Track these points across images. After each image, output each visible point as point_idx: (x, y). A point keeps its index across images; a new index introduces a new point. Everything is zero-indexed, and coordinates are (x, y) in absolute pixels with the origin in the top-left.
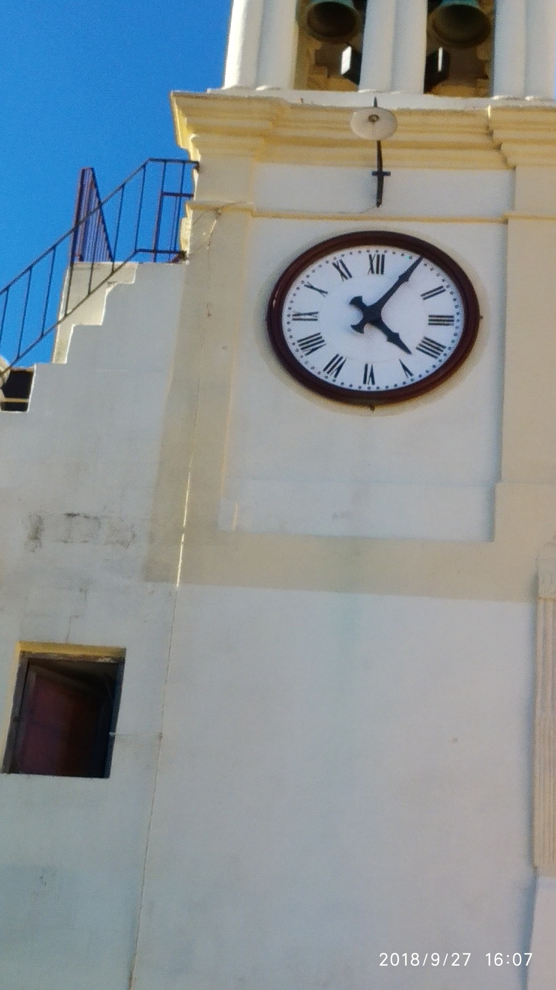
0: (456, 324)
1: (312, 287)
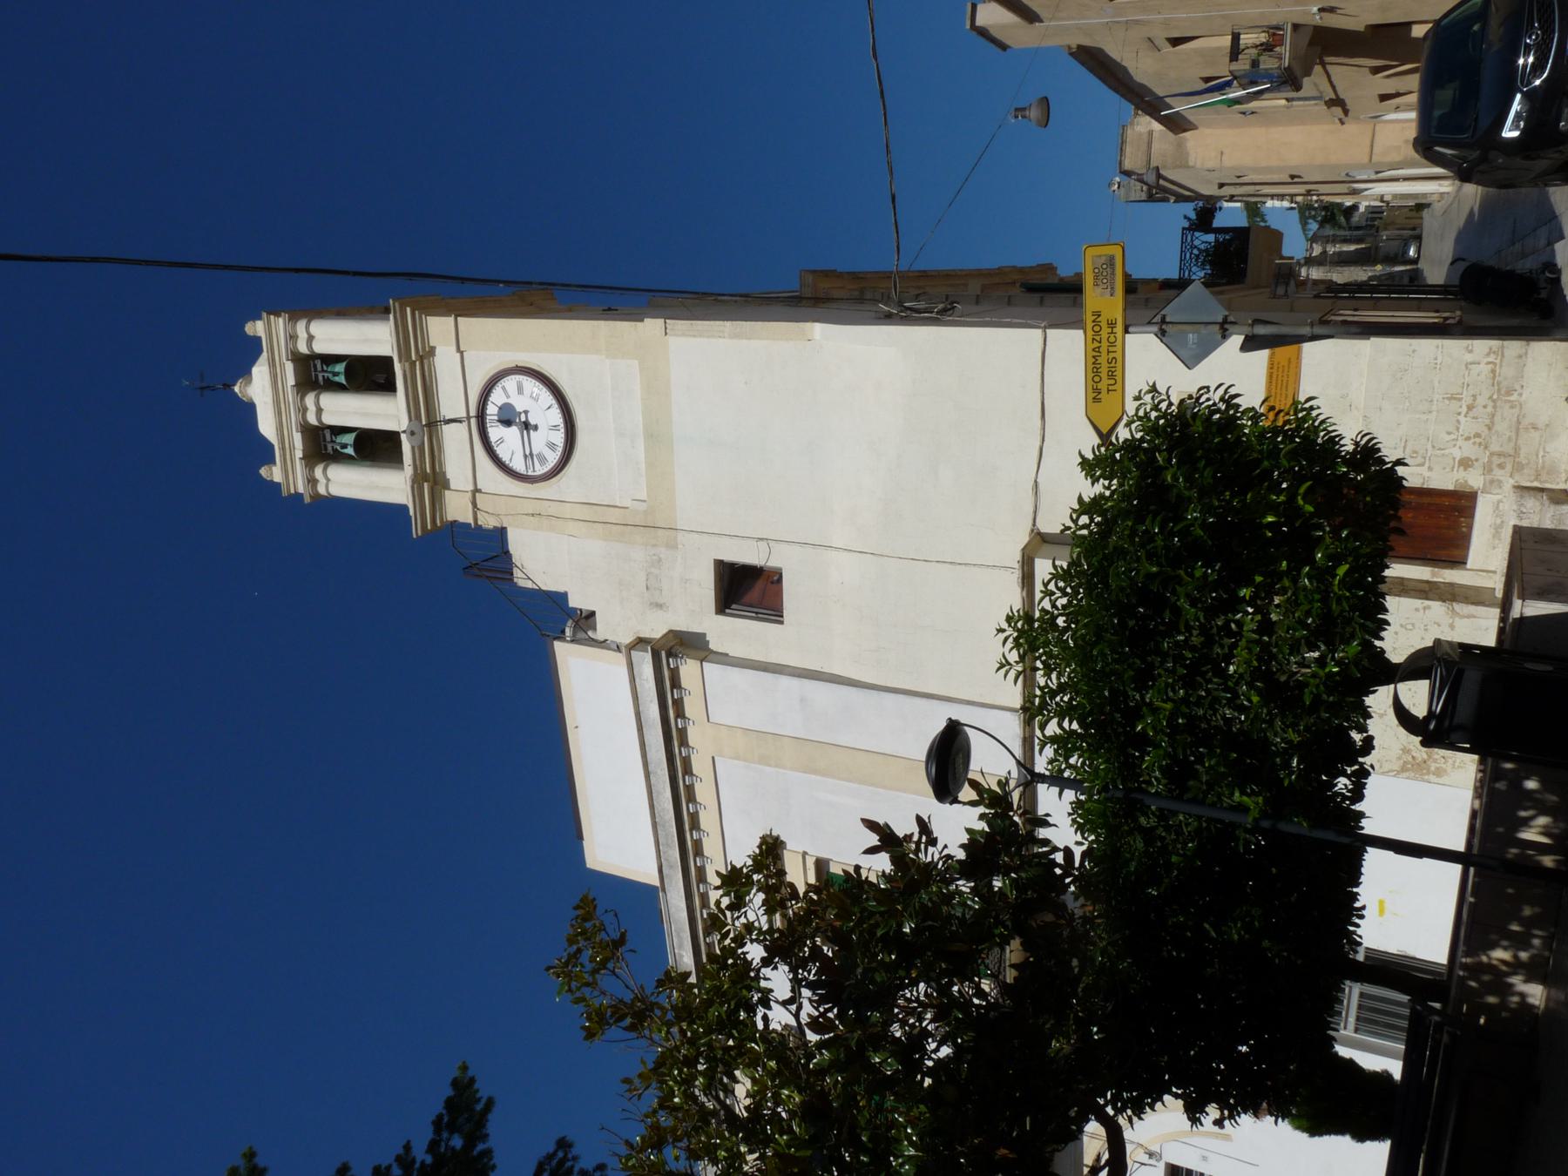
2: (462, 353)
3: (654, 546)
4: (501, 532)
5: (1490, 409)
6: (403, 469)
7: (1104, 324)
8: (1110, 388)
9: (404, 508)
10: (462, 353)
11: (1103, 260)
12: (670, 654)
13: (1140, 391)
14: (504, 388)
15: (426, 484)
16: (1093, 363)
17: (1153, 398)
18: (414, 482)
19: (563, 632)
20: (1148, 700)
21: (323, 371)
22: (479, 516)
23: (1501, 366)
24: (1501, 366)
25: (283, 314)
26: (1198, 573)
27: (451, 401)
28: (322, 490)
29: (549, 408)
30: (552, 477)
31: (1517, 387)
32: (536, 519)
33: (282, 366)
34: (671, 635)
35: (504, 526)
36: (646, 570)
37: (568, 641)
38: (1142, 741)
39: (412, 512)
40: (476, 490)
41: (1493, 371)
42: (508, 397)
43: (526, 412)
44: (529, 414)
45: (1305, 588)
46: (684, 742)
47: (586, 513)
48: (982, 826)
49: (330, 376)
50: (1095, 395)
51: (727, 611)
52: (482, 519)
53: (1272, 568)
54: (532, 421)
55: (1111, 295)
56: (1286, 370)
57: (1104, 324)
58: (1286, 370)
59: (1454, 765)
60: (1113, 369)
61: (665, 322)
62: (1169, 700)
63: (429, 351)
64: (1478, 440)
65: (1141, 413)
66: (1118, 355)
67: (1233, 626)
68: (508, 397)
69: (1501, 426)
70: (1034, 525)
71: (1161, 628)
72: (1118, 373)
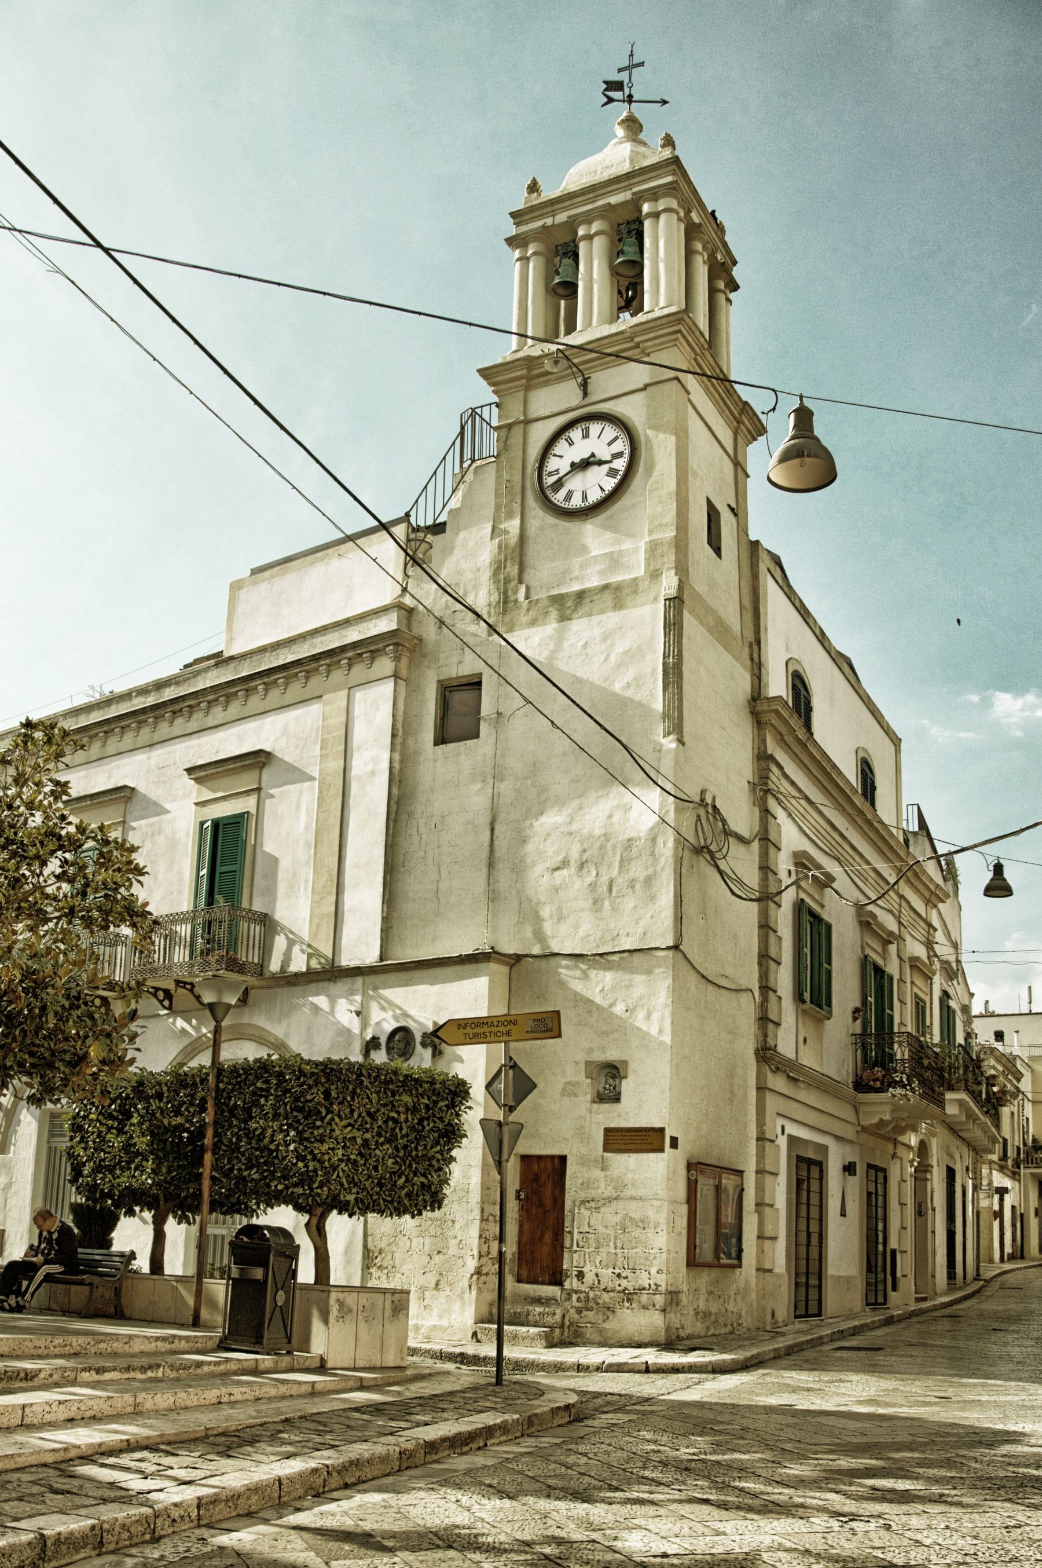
14: (616, 438)
33: (628, 187)
41: (644, 1289)
57: (508, 1028)
69: (606, 1297)
72: (476, 1040)
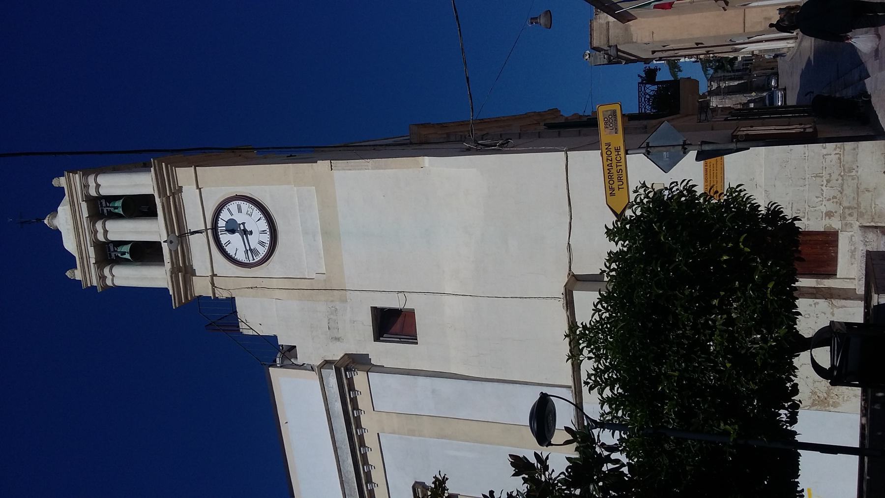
0: (240, 203)
1: (236, 254)
2: (200, 189)
3: (332, 301)
4: (232, 300)
5: (840, 181)
6: (164, 265)
7: (613, 150)
8: (620, 187)
9: (167, 290)
10: (200, 189)
11: (609, 113)
12: (346, 370)
13: (637, 187)
14: (229, 209)
15: (180, 274)
16: (609, 173)
17: (645, 191)
18: (172, 273)
19: (275, 361)
20: (663, 372)
21: (107, 206)
22: (216, 291)
23: (843, 156)
24: (843, 156)
25: (78, 172)
26: (687, 293)
27: (194, 219)
28: (109, 283)
29: (259, 220)
30: (262, 264)
31: (855, 167)
32: (255, 290)
33: (79, 205)
34: (346, 357)
35: (233, 296)
36: (328, 317)
37: (278, 367)
38: (662, 396)
39: (171, 293)
40: (214, 275)
41: (840, 159)
42: (232, 215)
43: (243, 224)
44: (245, 224)
45: (750, 296)
46: (359, 426)
47: (287, 284)
48: (576, 455)
49: (112, 209)
50: (611, 192)
51: (381, 339)
52: (218, 293)
53: (729, 286)
54: (249, 229)
55: (616, 133)
56: (715, 165)
57: (613, 150)
58: (715, 165)
59: (843, 399)
60: (621, 176)
61: (331, 162)
62: (676, 370)
63: (178, 190)
64: (835, 200)
65: (638, 200)
66: (623, 168)
67: (710, 322)
68: (232, 215)
69: (848, 191)
70: (570, 270)
71: (668, 327)
72: (624, 178)
